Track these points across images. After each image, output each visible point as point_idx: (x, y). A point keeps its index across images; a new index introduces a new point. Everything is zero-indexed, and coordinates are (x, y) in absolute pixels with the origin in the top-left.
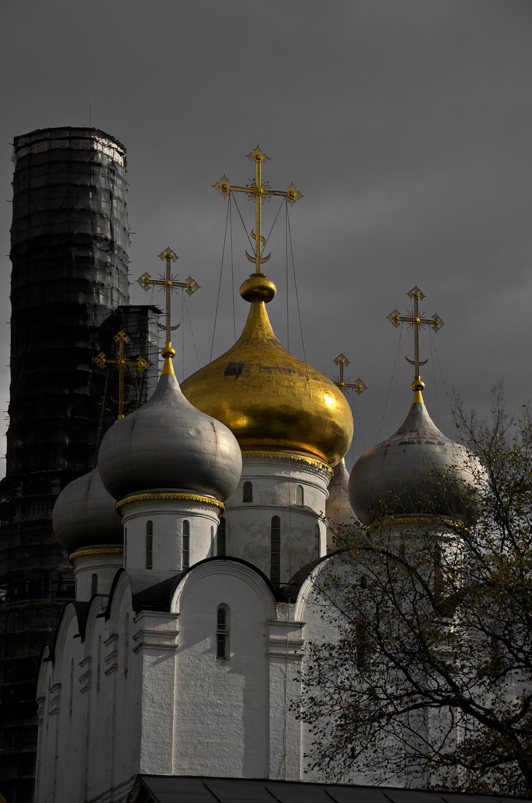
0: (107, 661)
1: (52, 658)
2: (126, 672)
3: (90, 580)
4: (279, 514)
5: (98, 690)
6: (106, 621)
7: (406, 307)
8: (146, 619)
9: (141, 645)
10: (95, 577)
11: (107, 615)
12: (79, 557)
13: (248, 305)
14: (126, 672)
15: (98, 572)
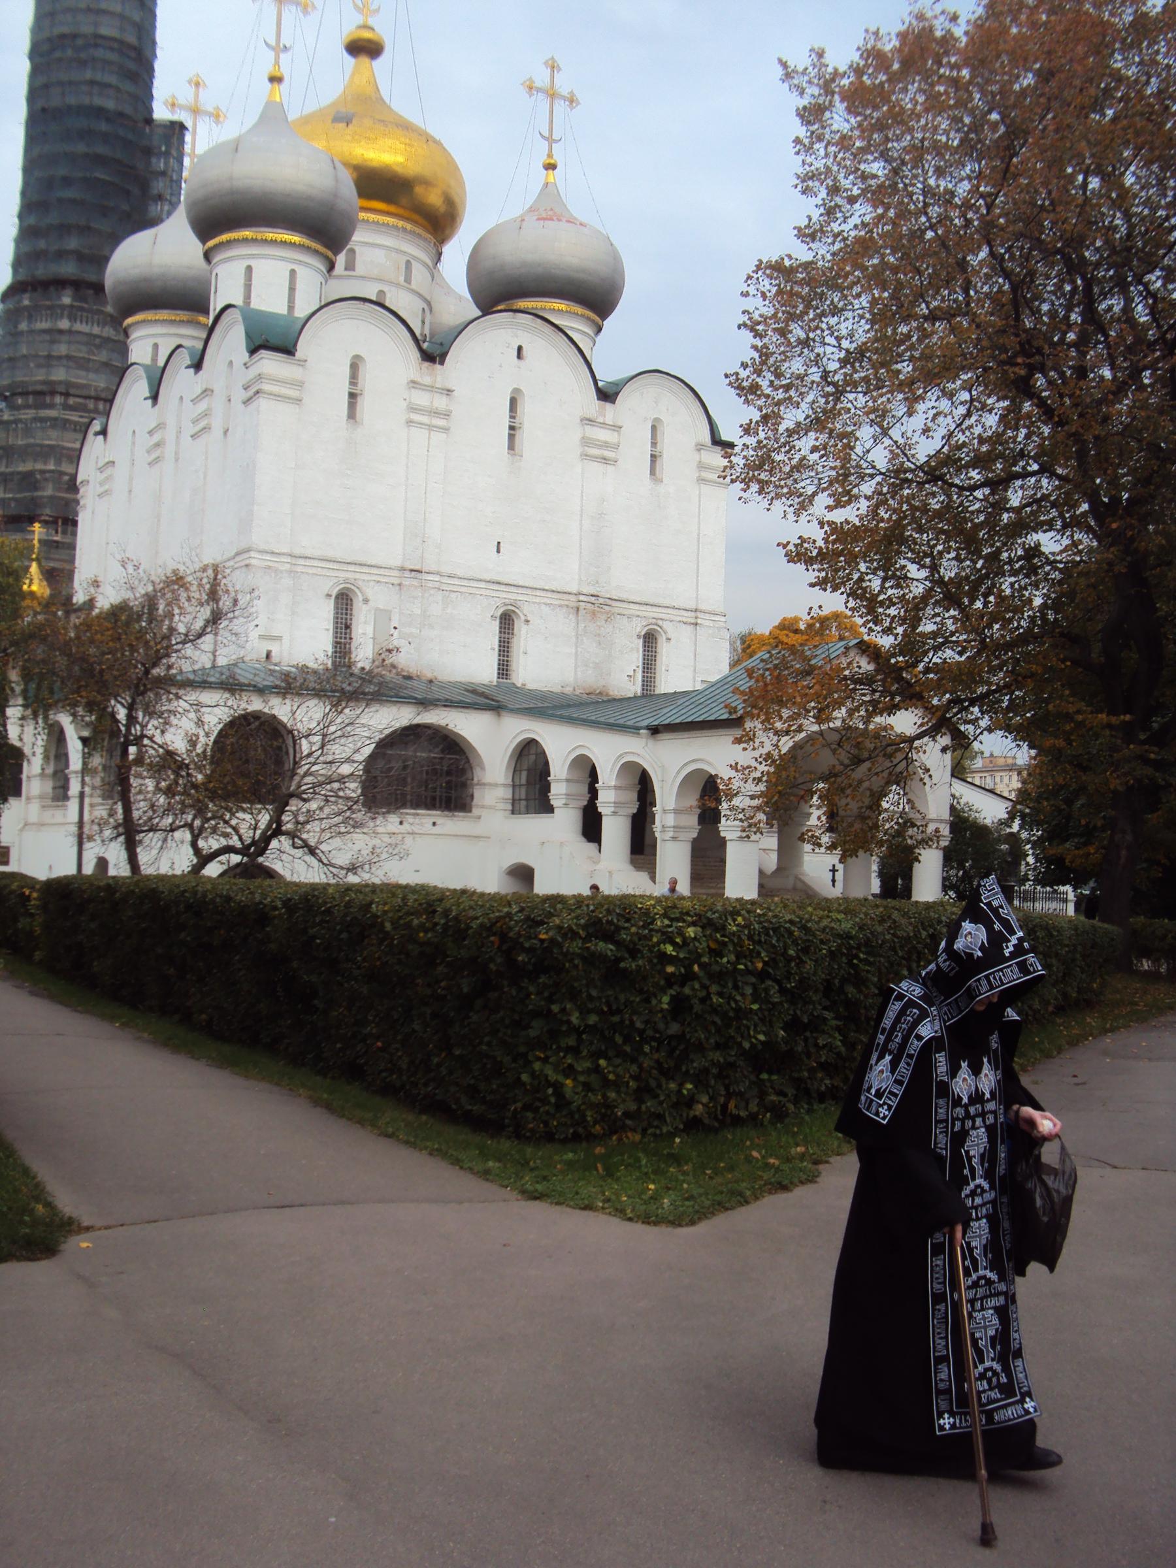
0: (195, 421)
1: (104, 432)
2: (226, 432)
3: (150, 349)
4: (386, 288)
5: (177, 460)
6: (196, 373)
7: (542, 78)
8: (265, 362)
9: (258, 392)
10: (156, 346)
11: (198, 366)
12: (138, 323)
13: (350, 61)
14: (226, 432)
15: (159, 340)
